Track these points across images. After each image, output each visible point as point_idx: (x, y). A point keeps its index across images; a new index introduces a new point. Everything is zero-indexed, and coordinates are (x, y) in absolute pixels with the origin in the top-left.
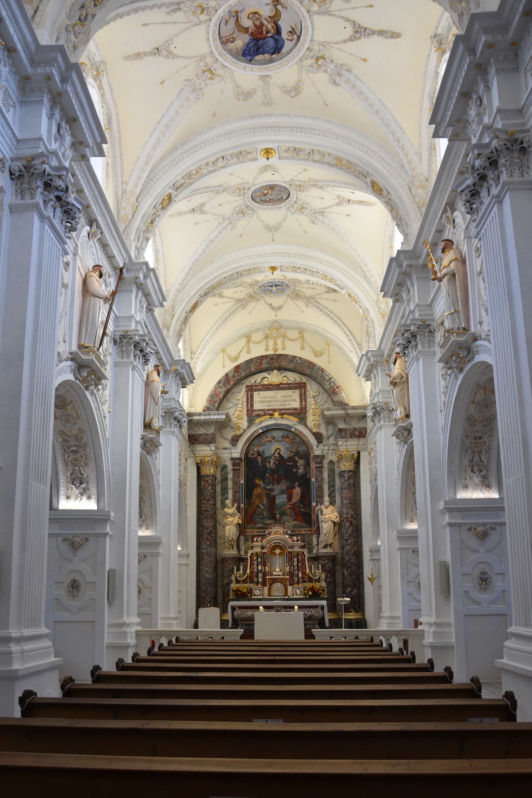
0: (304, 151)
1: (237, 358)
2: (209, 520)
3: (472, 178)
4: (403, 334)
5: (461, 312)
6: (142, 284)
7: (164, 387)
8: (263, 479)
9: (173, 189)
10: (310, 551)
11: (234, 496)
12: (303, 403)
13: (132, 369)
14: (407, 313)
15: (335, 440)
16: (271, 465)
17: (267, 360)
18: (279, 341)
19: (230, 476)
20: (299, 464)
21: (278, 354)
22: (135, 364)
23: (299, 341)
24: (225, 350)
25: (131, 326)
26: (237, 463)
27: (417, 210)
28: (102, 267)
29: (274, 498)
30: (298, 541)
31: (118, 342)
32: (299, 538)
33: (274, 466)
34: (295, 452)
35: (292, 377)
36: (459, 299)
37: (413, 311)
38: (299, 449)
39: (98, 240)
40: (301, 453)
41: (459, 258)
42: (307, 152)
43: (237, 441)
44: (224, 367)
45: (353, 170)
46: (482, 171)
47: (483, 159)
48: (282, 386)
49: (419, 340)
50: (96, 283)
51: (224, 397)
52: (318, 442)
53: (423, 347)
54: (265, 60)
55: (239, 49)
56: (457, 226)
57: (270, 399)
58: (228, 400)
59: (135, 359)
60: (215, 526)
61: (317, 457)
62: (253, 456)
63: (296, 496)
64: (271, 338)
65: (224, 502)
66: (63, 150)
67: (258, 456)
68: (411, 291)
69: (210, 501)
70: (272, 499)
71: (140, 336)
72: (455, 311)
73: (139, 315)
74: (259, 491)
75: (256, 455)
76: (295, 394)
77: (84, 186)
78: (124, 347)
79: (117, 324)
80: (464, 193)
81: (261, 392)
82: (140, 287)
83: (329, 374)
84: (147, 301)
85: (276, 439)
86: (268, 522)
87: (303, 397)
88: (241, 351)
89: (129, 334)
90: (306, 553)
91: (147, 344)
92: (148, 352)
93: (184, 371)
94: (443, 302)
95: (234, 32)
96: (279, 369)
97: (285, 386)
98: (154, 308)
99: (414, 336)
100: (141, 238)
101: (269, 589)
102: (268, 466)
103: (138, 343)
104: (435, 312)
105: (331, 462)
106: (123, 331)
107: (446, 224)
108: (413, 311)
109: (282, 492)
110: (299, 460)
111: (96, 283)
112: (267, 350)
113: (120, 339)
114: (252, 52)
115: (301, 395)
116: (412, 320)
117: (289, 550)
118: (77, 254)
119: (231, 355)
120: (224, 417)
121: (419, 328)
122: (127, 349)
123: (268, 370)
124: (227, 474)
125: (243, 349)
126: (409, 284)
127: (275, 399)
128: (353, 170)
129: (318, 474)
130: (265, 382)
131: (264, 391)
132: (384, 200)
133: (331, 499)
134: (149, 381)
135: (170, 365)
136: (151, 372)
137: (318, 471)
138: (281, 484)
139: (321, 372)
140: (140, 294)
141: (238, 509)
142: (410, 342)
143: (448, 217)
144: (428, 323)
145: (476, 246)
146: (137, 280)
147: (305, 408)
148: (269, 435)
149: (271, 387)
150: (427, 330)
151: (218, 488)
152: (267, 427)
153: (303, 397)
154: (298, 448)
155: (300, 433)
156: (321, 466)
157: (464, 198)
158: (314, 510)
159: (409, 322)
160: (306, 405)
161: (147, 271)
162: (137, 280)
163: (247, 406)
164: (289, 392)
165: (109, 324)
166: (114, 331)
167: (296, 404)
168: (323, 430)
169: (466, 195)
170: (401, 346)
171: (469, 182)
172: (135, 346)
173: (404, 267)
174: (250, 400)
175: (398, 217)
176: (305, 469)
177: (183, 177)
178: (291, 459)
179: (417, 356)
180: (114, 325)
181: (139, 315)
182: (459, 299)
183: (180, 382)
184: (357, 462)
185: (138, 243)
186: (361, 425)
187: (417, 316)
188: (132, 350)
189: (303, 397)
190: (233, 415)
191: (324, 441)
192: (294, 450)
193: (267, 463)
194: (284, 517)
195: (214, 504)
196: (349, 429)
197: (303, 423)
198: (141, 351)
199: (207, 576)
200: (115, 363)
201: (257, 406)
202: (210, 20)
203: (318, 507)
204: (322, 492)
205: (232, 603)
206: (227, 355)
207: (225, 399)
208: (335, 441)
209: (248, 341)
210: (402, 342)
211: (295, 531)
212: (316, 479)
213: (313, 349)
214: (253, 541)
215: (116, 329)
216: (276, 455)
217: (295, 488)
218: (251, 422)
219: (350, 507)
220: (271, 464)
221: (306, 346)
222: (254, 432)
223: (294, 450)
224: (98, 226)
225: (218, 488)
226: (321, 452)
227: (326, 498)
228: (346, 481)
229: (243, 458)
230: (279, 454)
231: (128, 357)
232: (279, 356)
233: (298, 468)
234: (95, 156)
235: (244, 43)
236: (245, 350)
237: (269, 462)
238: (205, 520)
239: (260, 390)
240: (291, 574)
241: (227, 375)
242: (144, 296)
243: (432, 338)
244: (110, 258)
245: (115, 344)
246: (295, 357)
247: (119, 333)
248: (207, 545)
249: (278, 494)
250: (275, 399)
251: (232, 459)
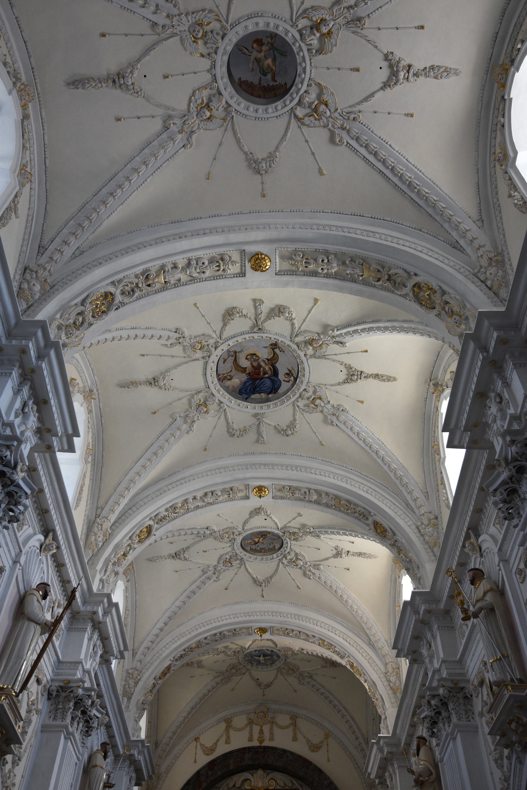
0: (300, 490)
1: (212, 750)
3: (507, 470)
4: (429, 702)
5: (511, 657)
6: (100, 623)
7: (109, 776)
9: (153, 520)
13: (65, 738)
14: (430, 675)
18: (266, 729)
21: (264, 747)
22: (71, 730)
23: (291, 729)
24: (199, 738)
25: (75, 674)
27: (429, 550)
28: (49, 585)
31: (54, 696)
36: (506, 641)
37: (439, 670)
39: (53, 556)
41: (495, 587)
42: (302, 491)
44: (195, 761)
45: (353, 511)
46: (511, 485)
47: (519, 445)
49: (452, 709)
50: (36, 603)
53: (459, 719)
54: (262, 399)
55: (236, 387)
56: (485, 554)
59: (72, 724)
64: (257, 724)
66: (23, 428)
71: (85, 689)
72: (502, 655)
73: (89, 663)
77: (45, 485)
78: (61, 703)
79: (59, 671)
80: (499, 491)
82: (93, 616)
84: (104, 647)
88: (218, 740)
89: (71, 685)
91: (93, 703)
92: (92, 715)
93: (141, 758)
94: (481, 645)
95: (231, 371)
98: (112, 658)
99: (445, 704)
100: (109, 570)
103: (81, 700)
104: (468, 671)
106: (63, 681)
107: (470, 554)
108: (439, 670)
111: (36, 603)
112: (250, 739)
113: (58, 691)
114: (248, 390)
116: (439, 680)
118: (19, 562)
119: (206, 745)
121: (450, 692)
122: (64, 708)
123: (252, 768)
125: (221, 737)
128: (353, 511)
132: (390, 542)
134: (91, 765)
135: (124, 747)
136: (95, 752)
140: (96, 636)
142: (439, 713)
143: (472, 544)
144: (461, 685)
145: (517, 568)
146: (94, 616)
150: (460, 695)
157: (498, 497)
159: (435, 684)
161: (109, 606)
162: (94, 616)
165: (42, 660)
166: (52, 680)
169: (502, 494)
170: (427, 720)
171: (504, 476)
172: (76, 704)
175: (408, 560)
177: (167, 510)
179: (452, 733)
180: (53, 671)
181: (89, 663)
182: (506, 641)
183: (134, 775)
185: (104, 575)
187: (444, 675)
188: (70, 708)
198: (84, 713)
200: (43, 726)
202: (209, 357)
206: (201, 745)
209: (229, 727)
210: (430, 714)
213: (308, 741)
215: (55, 678)
221: (299, 736)
224: (55, 538)
231: (63, 718)
234: (62, 450)
235: (241, 382)
236: (224, 738)
241: (198, 773)
242: (101, 639)
243: (469, 706)
244: (64, 581)
245: (49, 699)
246: (285, 751)
247: (57, 684)
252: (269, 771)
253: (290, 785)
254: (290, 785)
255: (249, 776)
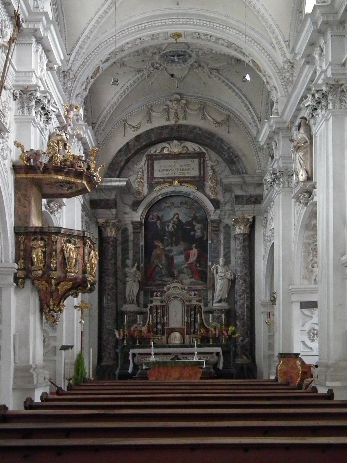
2: (110, 278)
8: (162, 241)
10: (206, 305)
11: (134, 256)
12: (202, 172)
15: (232, 206)
16: (169, 228)
17: (168, 130)
19: (131, 238)
20: (196, 228)
26: (138, 226)
29: (172, 258)
30: (195, 295)
32: (196, 292)
33: (173, 229)
34: (192, 217)
35: (192, 147)
38: (197, 215)
40: (199, 218)
43: (138, 206)
48: (181, 155)
51: (125, 165)
52: (216, 208)
57: (169, 168)
58: (128, 168)
60: (116, 284)
61: (213, 221)
62: (153, 220)
63: (193, 256)
65: (125, 261)
67: (157, 220)
68: (324, 50)
69: (111, 260)
70: (170, 260)
74: (158, 252)
75: (155, 220)
76: (195, 163)
81: (160, 161)
83: (228, 145)
85: (175, 205)
86: (166, 279)
87: (202, 166)
90: (202, 306)
96: (180, 139)
97: (184, 155)
101: (168, 338)
102: (167, 229)
105: (227, 226)
109: (180, 253)
110: (197, 224)
115: (200, 164)
117: (188, 303)
120: (125, 183)
123: (168, 140)
124: (127, 236)
126: (322, 43)
127: (174, 168)
129: (215, 236)
130: (165, 152)
131: (163, 159)
133: (226, 260)
137: (214, 234)
138: (179, 246)
139: (219, 142)
141: (138, 268)
147: (204, 177)
148: (169, 201)
149: (170, 156)
151: (119, 249)
152: (167, 194)
153: (202, 166)
154: (196, 213)
155: (198, 200)
156: (217, 229)
158: (210, 269)
160: (204, 174)
163: (148, 174)
164: (189, 161)
167: (195, 173)
168: (220, 197)
173: (320, 24)
174: (151, 169)
176: (202, 232)
178: (189, 223)
184: (252, 226)
186: (257, 192)
189: (202, 166)
190: (134, 182)
191: (221, 206)
192: (192, 215)
193: (166, 227)
194: (182, 275)
195: (116, 263)
196: (246, 196)
197: (202, 190)
199: (108, 327)
201: (157, 174)
203: (213, 267)
204: (218, 253)
205: (132, 351)
207: (126, 167)
208: (231, 207)
211: (191, 288)
212: (212, 242)
214: (152, 296)
216: (175, 219)
217: (192, 249)
218: (151, 188)
219: (244, 266)
220: (170, 228)
222: (154, 198)
223: (192, 215)
225: (119, 249)
226: (218, 217)
227: (221, 260)
228: (240, 243)
229: (143, 222)
230: (178, 218)
232: (180, 126)
233: (195, 231)
237: (168, 226)
238: (107, 278)
239: (160, 159)
240: (188, 325)
248: (108, 299)
249: (176, 255)
250: (174, 168)
251: (132, 223)
252: (183, 141)
253: (199, 150)
254: (199, 150)
255: (167, 145)
